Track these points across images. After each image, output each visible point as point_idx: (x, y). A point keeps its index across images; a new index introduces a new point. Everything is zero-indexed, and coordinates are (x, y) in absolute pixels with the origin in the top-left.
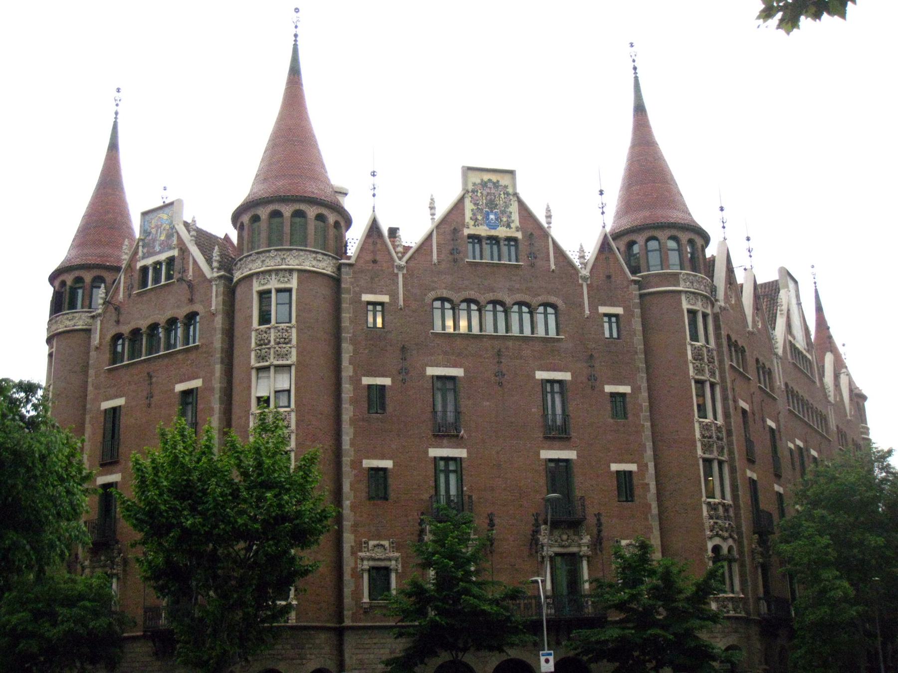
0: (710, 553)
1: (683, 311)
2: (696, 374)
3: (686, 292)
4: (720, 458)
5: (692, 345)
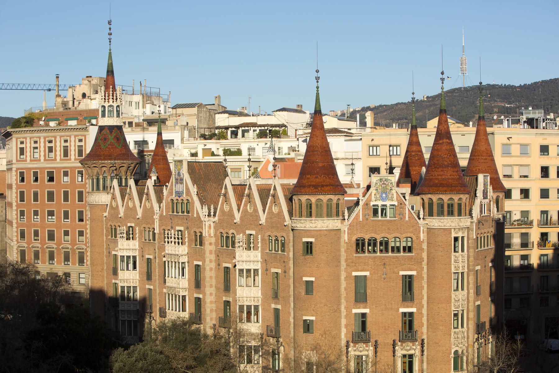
0: (452, 355)
2: (455, 270)
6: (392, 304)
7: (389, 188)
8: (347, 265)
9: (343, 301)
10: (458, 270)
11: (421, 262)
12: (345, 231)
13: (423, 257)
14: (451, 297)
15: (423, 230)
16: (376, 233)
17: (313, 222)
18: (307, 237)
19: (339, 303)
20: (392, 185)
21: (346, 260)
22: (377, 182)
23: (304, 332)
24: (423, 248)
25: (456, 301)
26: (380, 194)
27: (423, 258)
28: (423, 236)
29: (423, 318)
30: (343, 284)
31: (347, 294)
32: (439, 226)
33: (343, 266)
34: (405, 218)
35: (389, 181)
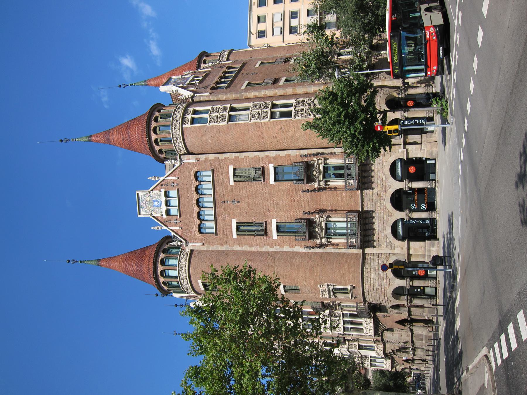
1: (192, 127)
2: (225, 120)
3: (182, 124)
4: (270, 108)
5: (210, 122)
6: (265, 193)
7: (149, 198)
8: (226, 244)
9: (264, 249)
10: (226, 116)
11: (219, 160)
12: (192, 245)
13: (213, 158)
14: (255, 123)
15: (186, 160)
16: (192, 212)
17: (182, 281)
18: (199, 286)
19: (267, 253)
20: (146, 195)
21: (221, 245)
22: (144, 211)
23: (299, 293)
24: (205, 158)
25: (258, 117)
26: (156, 208)
27: (215, 158)
28: (193, 159)
29: (281, 156)
30: (246, 248)
31: (257, 245)
32: (181, 142)
33: (228, 248)
34: (176, 180)
35: (143, 198)
